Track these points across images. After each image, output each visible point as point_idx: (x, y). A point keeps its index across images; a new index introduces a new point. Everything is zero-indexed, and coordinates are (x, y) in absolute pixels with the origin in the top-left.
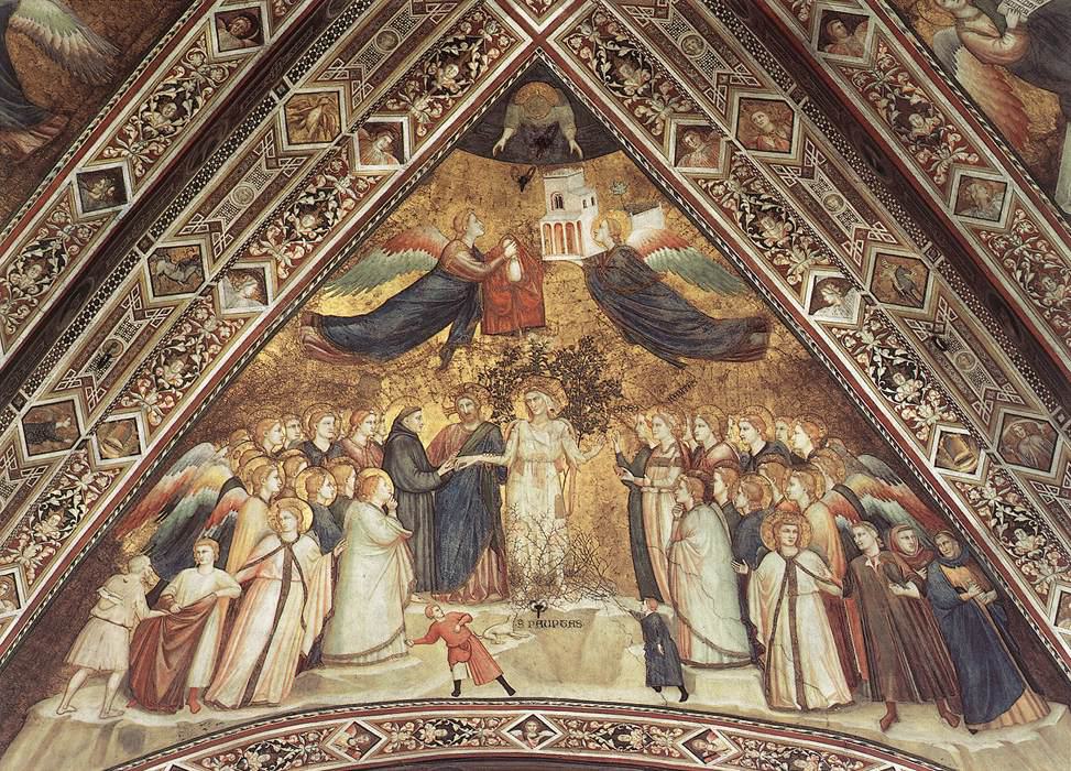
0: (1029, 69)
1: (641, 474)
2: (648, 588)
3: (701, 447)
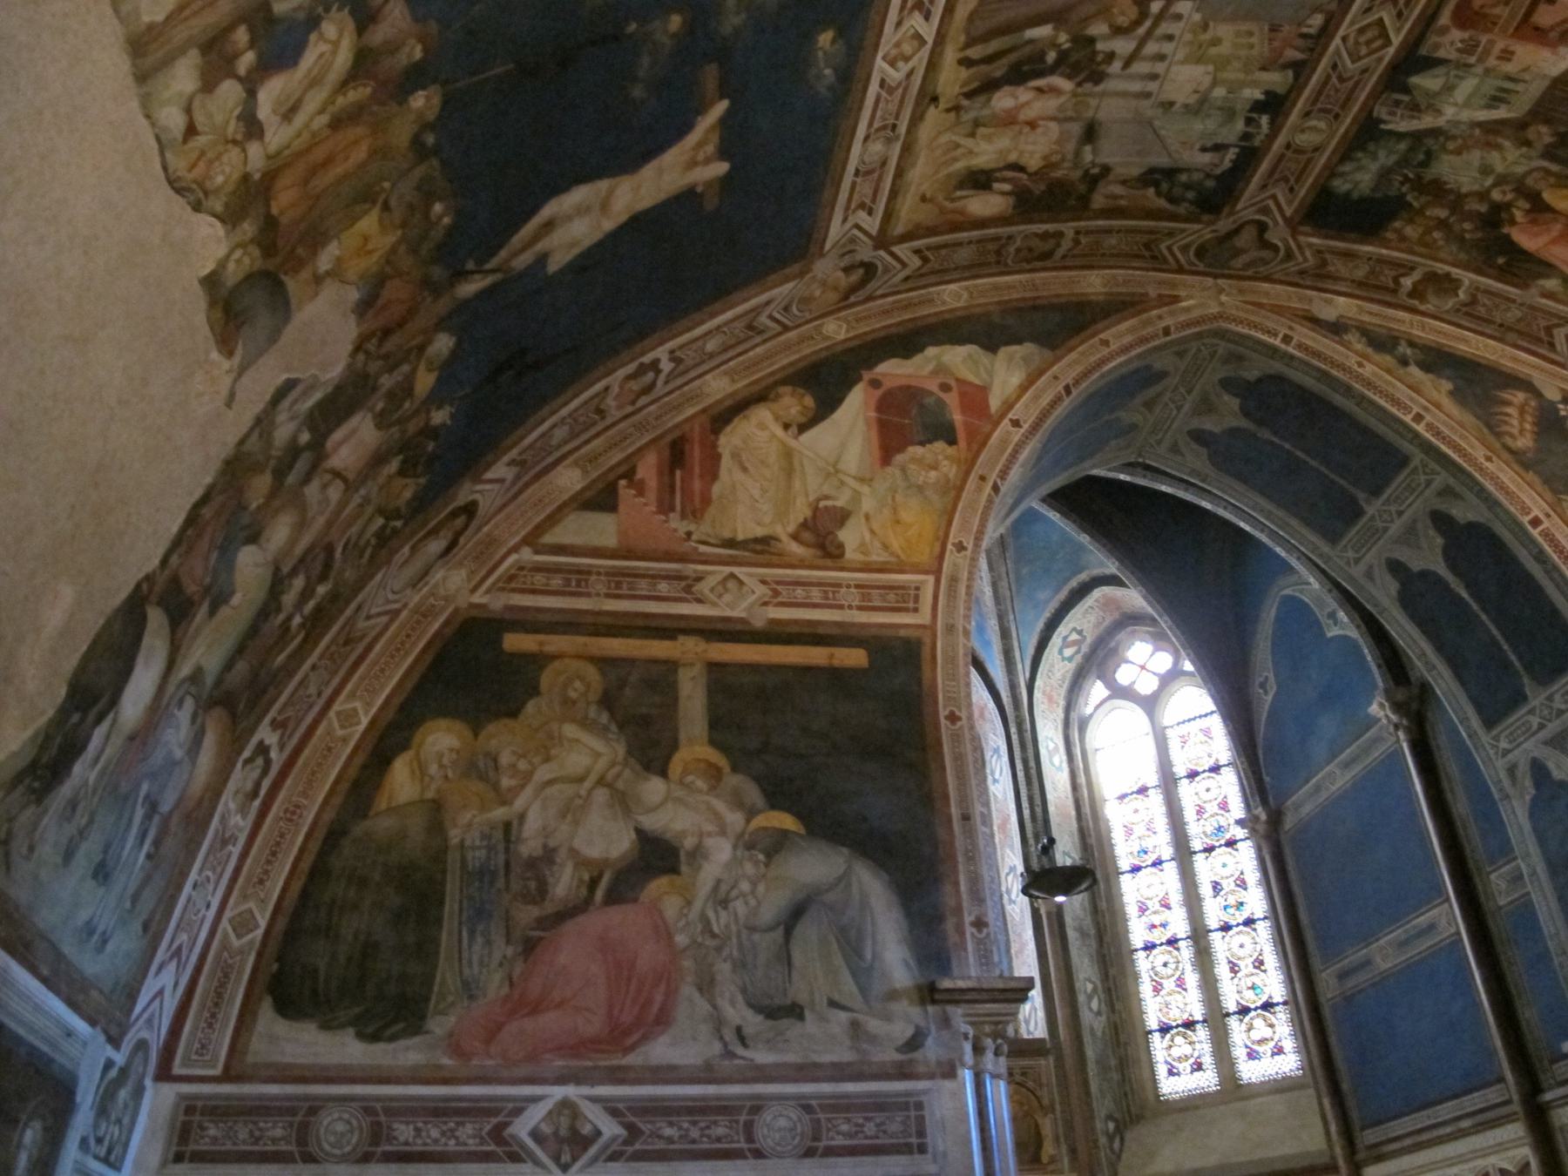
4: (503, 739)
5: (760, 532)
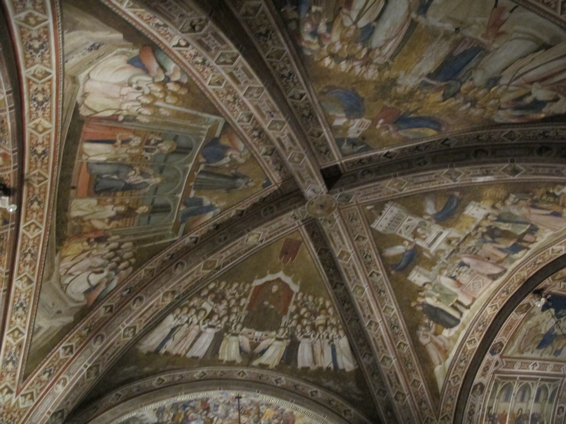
0: (226, 148)
1: (387, 63)
2: (413, 24)
3: (361, 66)
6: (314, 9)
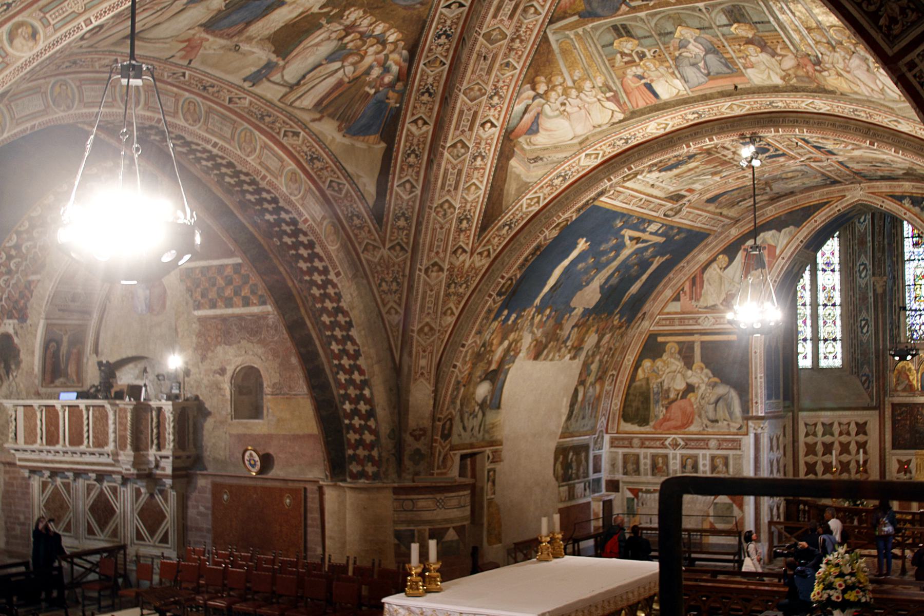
4: (659, 363)
5: (713, 303)
6: (372, 91)
